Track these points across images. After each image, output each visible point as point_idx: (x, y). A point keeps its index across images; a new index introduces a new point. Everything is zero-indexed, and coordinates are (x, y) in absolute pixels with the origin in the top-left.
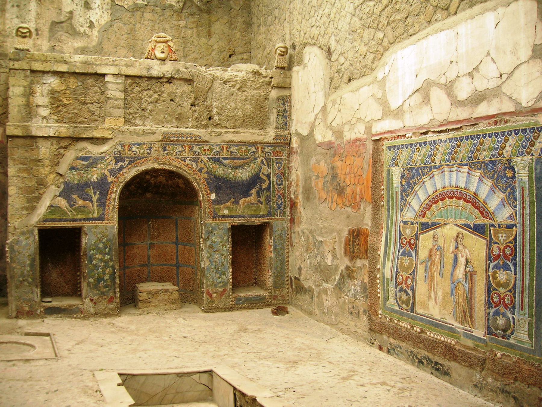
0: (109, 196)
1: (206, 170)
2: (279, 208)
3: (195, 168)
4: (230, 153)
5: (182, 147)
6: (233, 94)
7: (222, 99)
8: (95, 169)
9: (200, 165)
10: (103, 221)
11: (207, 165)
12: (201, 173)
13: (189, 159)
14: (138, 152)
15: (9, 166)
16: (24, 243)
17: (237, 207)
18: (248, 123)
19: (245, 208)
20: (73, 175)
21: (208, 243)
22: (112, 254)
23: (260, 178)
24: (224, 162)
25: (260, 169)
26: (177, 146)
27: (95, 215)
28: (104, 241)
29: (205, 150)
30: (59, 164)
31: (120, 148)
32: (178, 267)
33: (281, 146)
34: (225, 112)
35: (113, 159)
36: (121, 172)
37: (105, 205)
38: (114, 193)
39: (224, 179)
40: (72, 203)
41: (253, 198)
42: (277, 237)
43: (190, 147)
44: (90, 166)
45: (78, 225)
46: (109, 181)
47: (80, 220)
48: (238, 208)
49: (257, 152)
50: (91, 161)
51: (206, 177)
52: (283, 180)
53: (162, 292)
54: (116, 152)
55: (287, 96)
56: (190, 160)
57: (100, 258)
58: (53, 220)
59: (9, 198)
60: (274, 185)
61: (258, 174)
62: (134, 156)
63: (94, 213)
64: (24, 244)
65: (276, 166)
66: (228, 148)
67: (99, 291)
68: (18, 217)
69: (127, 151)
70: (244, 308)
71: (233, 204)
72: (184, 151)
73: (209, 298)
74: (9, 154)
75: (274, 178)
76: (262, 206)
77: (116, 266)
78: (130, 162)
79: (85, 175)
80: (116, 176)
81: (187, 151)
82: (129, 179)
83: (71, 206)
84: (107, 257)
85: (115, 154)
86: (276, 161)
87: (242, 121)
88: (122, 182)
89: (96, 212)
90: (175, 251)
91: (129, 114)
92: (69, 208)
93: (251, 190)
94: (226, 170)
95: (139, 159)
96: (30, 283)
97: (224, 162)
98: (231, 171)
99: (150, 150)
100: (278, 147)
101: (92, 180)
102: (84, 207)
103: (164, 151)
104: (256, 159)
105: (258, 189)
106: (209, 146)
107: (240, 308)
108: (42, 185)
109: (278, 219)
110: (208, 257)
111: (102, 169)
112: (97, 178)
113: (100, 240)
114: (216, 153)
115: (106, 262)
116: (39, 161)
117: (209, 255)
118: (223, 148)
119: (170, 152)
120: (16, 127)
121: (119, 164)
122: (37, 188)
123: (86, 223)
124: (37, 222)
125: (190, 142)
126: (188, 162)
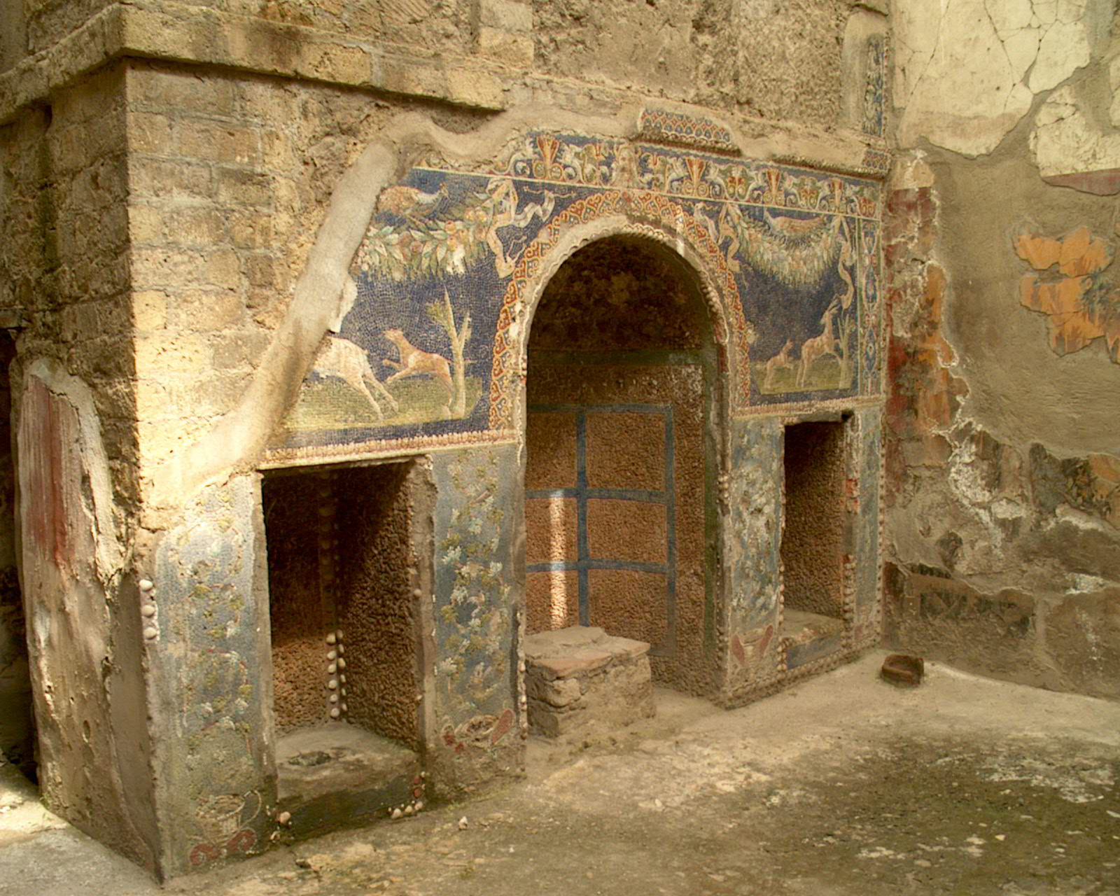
0: (500, 332)
1: (738, 245)
2: (870, 369)
4: (783, 196)
5: (684, 163)
6: (778, 12)
7: (758, 21)
8: (459, 225)
9: (726, 230)
10: (482, 429)
11: (740, 231)
12: (726, 255)
13: (700, 205)
14: (579, 169)
15: (131, 198)
17: (796, 367)
18: (803, 108)
20: (387, 244)
23: (840, 280)
24: (777, 223)
26: (671, 161)
27: (461, 411)
29: (733, 178)
30: (332, 197)
31: (529, 151)
33: (873, 185)
34: (762, 63)
35: (512, 190)
36: (535, 241)
37: (490, 367)
40: (386, 362)
41: (823, 342)
43: (701, 166)
44: (441, 212)
46: (502, 275)
47: (412, 431)
48: (800, 370)
49: (833, 197)
51: (737, 269)
52: (877, 284)
54: (520, 165)
55: (883, 38)
56: (704, 211)
57: (474, 575)
60: (861, 299)
61: (835, 263)
62: (569, 183)
63: (456, 398)
66: (780, 179)
67: (472, 700)
68: (180, 432)
69: (548, 161)
70: (803, 676)
71: (791, 358)
72: (689, 177)
73: (738, 663)
74: (134, 144)
75: (862, 280)
76: (842, 363)
78: (560, 205)
79: (427, 249)
81: (695, 178)
82: (555, 270)
83: (382, 374)
85: (517, 173)
86: (864, 228)
87: (793, 98)
89: (463, 393)
91: (541, 29)
92: (375, 383)
93: (822, 314)
94: (776, 248)
95: (581, 194)
99: (609, 165)
100: (867, 185)
101: (449, 269)
102: (424, 377)
103: (642, 175)
104: (830, 218)
106: (741, 168)
109: (869, 401)
111: (481, 227)
114: (756, 193)
115: (492, 588)
118: (770, 179)
119: (658, 180)
120: (168, 18)
121: (530, 210)
123: (430, 444)
125: (704, 149)
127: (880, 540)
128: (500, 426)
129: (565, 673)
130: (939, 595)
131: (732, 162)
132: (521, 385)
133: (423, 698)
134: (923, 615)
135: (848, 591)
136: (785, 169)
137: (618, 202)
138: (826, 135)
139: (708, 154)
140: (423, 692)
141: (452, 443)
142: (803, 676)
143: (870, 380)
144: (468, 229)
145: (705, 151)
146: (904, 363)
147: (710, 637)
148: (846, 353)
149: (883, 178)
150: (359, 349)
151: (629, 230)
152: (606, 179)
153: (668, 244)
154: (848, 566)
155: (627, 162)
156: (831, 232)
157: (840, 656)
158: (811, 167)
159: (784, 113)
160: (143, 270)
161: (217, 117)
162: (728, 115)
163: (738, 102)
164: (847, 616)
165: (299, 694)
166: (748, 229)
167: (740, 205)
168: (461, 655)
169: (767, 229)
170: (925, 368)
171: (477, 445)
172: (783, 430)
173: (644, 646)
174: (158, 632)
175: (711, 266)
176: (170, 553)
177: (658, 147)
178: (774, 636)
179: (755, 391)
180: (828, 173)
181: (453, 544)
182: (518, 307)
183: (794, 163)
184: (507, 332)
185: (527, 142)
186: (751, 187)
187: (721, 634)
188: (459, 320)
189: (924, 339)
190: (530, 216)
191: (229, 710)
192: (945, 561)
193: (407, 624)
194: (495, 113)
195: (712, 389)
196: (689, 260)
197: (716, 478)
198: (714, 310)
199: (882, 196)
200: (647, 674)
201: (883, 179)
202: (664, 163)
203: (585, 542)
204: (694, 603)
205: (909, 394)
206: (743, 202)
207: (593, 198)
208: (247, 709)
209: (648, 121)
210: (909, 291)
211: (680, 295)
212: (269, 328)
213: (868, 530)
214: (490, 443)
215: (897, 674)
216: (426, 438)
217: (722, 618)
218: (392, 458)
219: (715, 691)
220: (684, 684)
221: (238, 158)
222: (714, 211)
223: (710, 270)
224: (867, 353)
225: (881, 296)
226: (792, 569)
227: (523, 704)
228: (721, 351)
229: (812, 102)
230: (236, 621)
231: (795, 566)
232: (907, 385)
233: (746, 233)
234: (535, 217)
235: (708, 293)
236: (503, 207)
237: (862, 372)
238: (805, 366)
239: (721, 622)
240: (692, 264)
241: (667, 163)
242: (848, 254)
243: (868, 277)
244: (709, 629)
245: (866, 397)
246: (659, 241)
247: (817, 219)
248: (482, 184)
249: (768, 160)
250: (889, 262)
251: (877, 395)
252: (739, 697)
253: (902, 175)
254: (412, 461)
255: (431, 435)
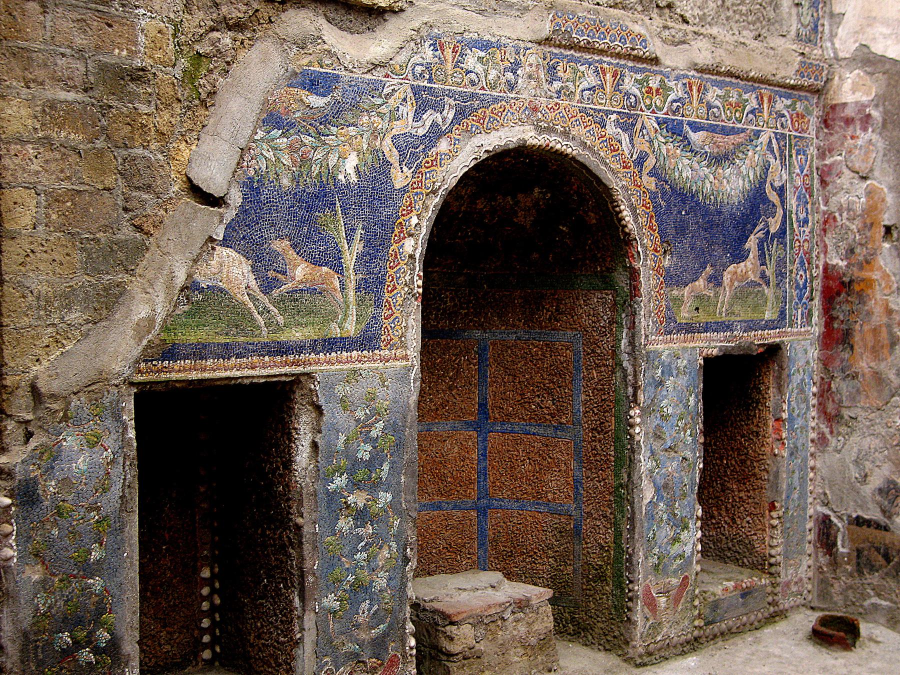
2: (800, 299)
3: (626, 152)
5: (596, 71)
11: (656, 145)
13: (614, 117)
14: (482, 76)
16: (81, 463)
17: (717, 295)
18: (730, 13)
19: (735, 297)
21: (654, 421)
22: (399, 483)
23: (765, 200)
24: (696, 137)
25: (766, 168)
26: (582, 68)
27: (351, 328)
28: (374, 433)
29: (651, 88)
30: (218, 98)
31: (428, 53)
32: (482, 512)
37: (382, 282)
38: (411, 235)
39: (693, 196)
40: (271, 274)
41: (748, 267)
42: (794, 395)
43: (615, 75)
45: (287, 370)
46: (397, 186)
47: (300, 348)
50: (338, 94)
51: (652, 187)
53: (513, 612)
54: (419, 69)
56: (617, 123)
57: (361, 505)
58: (200, 352)
59: (7, 245)
62: (470, 89)
64: (83, 467)
65: (796, 163)
68: (46, 341)
69: (449, 66)
71: (711, 285)
75: (792, 202)
76: (769, 292)
77: (409, 532)
78: (461, 114)
79: (319, 155)
80: (419, 166)
81: (608, 89)
82: (454, 182)
83: (267, 286)
84: (385, 497)
88: (434, 192)
89: (353, 310)
90: (475, 456)
94: (696, 165)
95: (485, 103)
96: (104, 651)
97: (696, 137)
98: (707, 170)
100: (800, 99)
101: (341, 177)
104: (757, 134)
105: (760, 235)
106: (659, 78)
107: (715, 636)
108: (148, 188)
110: (651, 471)
111: (376, 134)
112: (357, 169)
113: (365, 426)
114: (675, 105)
116: (138, 75)
117: (654, 463)
118: (692, 90)
121: (429, 117)
122: (127, 200)
124: (137, 362)
125: (618, 56)
126: (611, 129)
127: (811, 488)
128: (392, 346)
129: (460, 617)
130: (878, 550)
131: (649, 71)
132: (415, 306)
133: (303, 635)
134: (860, 573)
135: (775, 542)
136: (707, 80)
137: (525, 110)
138: (755, 44)
139: (622, 62)
140: (302, 629)
141: (340, 362)
142: (722, 634)
143: (800, 311)
144: (362, 135)
145: (620, 58)
146: (839, 294)
147: (620, 586)
148: (772, 279)
149: (818, 91)
150: (243, 259)
151: (535, 142)
152: (511, 87)
153: (579, 158)
154: (774, 514)
155: (534, 68)
156: (758, 148)
157: (766, 614)
158: (737, 77)
159: (709, 19)
160: (12, 167)
161: (94, 6)
162: (646, 19)
163: (658, 6)
164: (773, 570)
165: (168, 633)
166: (665, 144)
167: (657, 118)
168: (345, 590)
169: (686, 144)
170: (862, 297)
171: (367, 365)
172: (702, 362)
173: (548, 593)
174: (16, 554)
175: (624, 183)
176: (31, 467)
177: (569, 53)
178: (689, 588)
179: (671, 319)
180: (756, 85)
181: (339, 471)
182: (414, 221)
183: (719, 73)
184: (402, 246)
185: (427, 44)
186: (669, 99)
187: (631, 582)
188: (350, 233)
189: (861, 268)
190: (428, 124)
191: (89, 643)
192: (884, 512)
193: (289, 556)
194: (392, 11)
195: (623, 315)
196: (601, 176)
197: (627, 412)
198: (627, 231)
199: (817, 112)
200: (550, 623)
201: (818, 92)
202: (575, 71)
203: (485, 480)
204: (602, 548)
205: (844, 327)
206: (660, 115)
207: (497, 106)
208: (109, 641)
209: (557, 24)
210: (845, 214)
211: (590, 213)
212: (146, 234)
213: (796, 475)
214: (381, 364)
215: (831, 636)
216: (313, 355)
217: (631, 563)
218: (275, 376)
219: (623, 646)
220: (590, 637)
221: (117, 51)
222: (628, 124)
223: (623, 187)
224: (796, 279)
225: (815, 219)
226: (713, 517)
227: (411, 648)
228: (634, 274)
229: (741, 7)
230: (101, 545)
231: (716, 513)
232: (841, 318)
233: (664, 149)
234: (434, 124)
235: (621, 212)
236: (400, 112)
237: (791, 302)
238: (726, 294)
239: (631, 569)
240: (604, 181)
241: (579, 71)
242: (778, 175)
243: (799, 198)
244: (618, 577)
245: (796, 330)
246: (567, 155)
247: (742, 135)
248: (376, 88)
249: (689, 69)
250: (824, 183)
251: (809, 328)
252: (650, 654)
253: (840, 87)
254: (296, 381)
255: (318, 354)
